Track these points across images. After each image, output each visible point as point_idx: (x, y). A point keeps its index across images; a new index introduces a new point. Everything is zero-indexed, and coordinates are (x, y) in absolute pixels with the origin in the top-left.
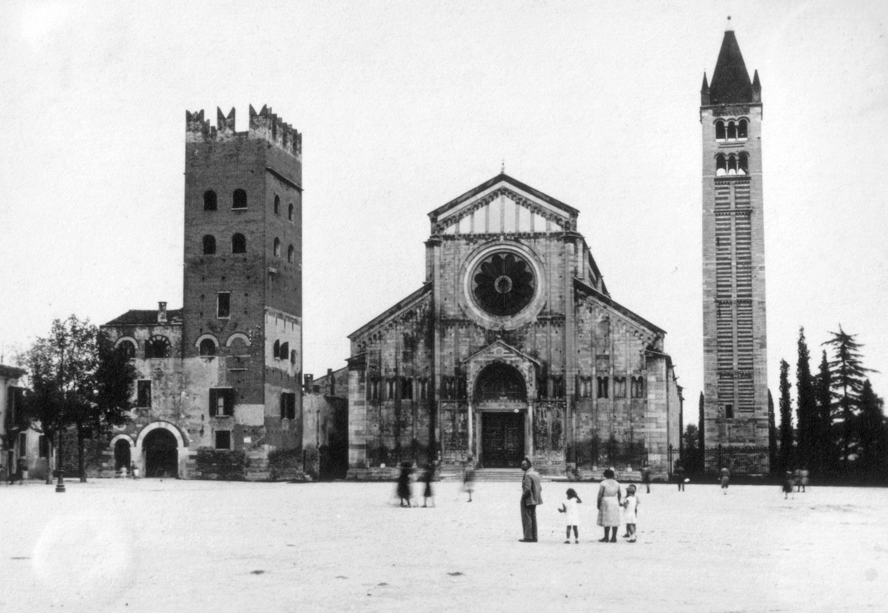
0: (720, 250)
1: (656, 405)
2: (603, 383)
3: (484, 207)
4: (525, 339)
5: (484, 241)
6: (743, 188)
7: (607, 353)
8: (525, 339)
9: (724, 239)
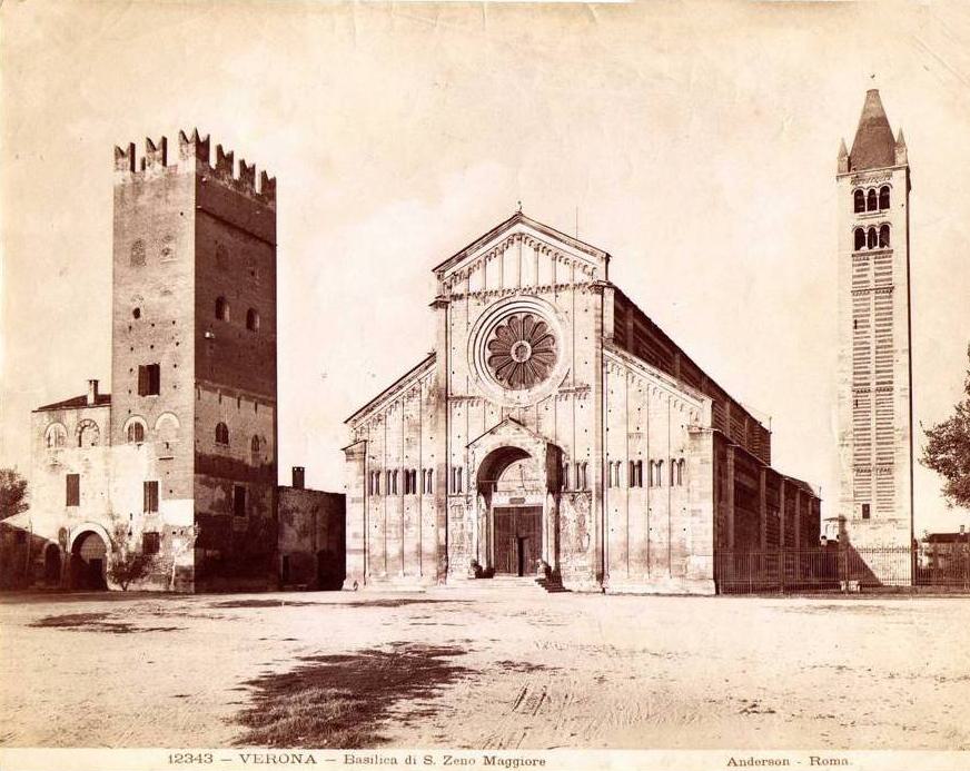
0: (857, 333)
1: (700, 494)
2: (635, 468)
3: (499, 257)
6: (885, 262)
9: (862, 321)
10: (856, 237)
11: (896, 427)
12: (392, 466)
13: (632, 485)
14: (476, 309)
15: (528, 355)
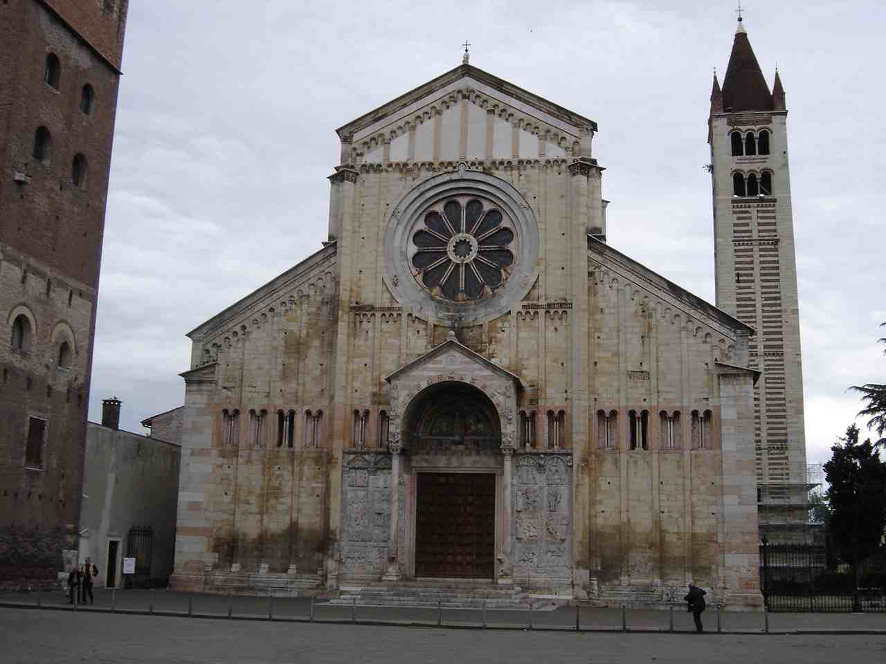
0: (740, 288)
3: (433, 119)
5: (430, 174)
7: (645, 368)
9: (747, 275)
10: (735, 182)
13: (633, 446)
14: (398, 189)
15: (473, 255)
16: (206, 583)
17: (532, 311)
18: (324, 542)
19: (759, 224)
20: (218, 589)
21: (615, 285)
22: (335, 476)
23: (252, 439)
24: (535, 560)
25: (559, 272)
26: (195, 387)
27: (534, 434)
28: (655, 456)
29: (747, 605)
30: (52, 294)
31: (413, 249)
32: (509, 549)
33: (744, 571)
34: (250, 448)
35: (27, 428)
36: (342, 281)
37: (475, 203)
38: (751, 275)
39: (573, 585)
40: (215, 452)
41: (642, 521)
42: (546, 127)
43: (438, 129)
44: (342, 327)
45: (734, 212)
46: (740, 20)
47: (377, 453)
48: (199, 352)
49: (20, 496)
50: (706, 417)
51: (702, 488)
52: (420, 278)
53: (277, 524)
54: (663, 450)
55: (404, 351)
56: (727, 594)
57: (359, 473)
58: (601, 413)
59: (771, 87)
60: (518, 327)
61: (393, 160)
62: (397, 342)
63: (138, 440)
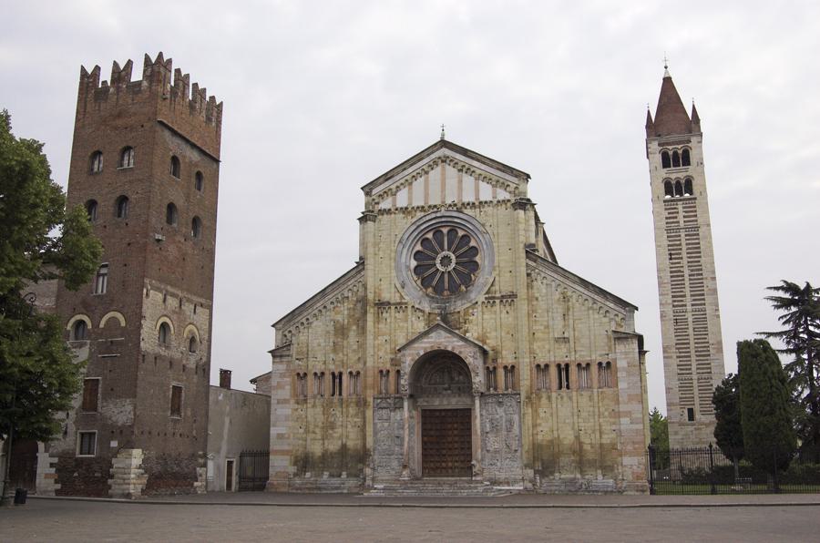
0: (672, 263)
4: (471, 322)
5: (423, 214)
7: (566, 335)
8: (471, 322)
9: (677, 254)
11: (711, 342)
12: (319, 368)
13: (560, 387)
14: (403, 224)
15: (453, 265)
16: (289, 486)
17: (491, 301)
18: (363, 456)
19: (684, 217)
20: (297, 489)
21: (545, 281)
22: (369, 413)
23: (316, 392)
24: (498, 464)
25: (509, 274)
26: (278, 360)
27: (496, 381)
28: (574, 393)
29: (637, 491)
30: (183, 307)
31: (414, 263)
32: (480, 457)
33: (635, 467)
34: (314, 397)
35: (171, 392)
36: (368, 287)
37: (453, 231)
38: (680, 254)
39: (523, 480)
40: (292, 401)
41: (568, 437)
42: (497, 178)
43: (426, 182)
44: (370, 318)
45: (666, 209)
46: (666, 67)
47: (395, 398)
48: (280, 337)
49: (168, 435)
50: (607, 367)
51: (606, 413)
52: (419, 282)
53: (333, 446)
54: (580, 388)
55: (410, 331)
56: (625, 484)
57: (384, 411)
58: (538, 366)
59: (690, 114)
60: (483, 313)
61: (399, 205)
62: (406, 325)
63: (245, 395)
